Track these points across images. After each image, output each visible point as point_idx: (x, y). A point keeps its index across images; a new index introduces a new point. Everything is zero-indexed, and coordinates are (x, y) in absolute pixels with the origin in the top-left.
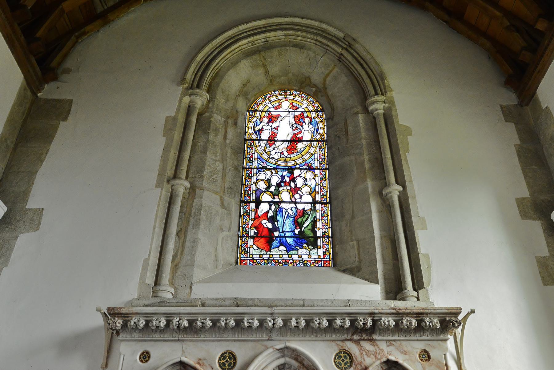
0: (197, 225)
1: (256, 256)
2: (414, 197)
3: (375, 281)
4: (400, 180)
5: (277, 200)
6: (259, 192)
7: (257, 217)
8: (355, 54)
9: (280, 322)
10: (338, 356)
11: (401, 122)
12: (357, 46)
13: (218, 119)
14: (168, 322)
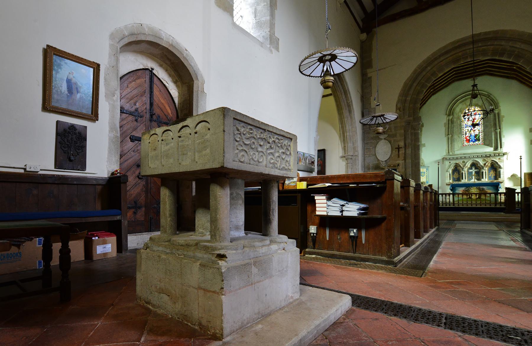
0: (454, 142)
1: (466, 144)
2: (503, 131)
3: (492, 147)
4: (500, 128)
5: (470, 133)
6: (466, 132)
7: (466, 137)
8: (491, 98)
11: (502, 115)
12: (491, 96)
13: (455, 120)
14: (453, 158)
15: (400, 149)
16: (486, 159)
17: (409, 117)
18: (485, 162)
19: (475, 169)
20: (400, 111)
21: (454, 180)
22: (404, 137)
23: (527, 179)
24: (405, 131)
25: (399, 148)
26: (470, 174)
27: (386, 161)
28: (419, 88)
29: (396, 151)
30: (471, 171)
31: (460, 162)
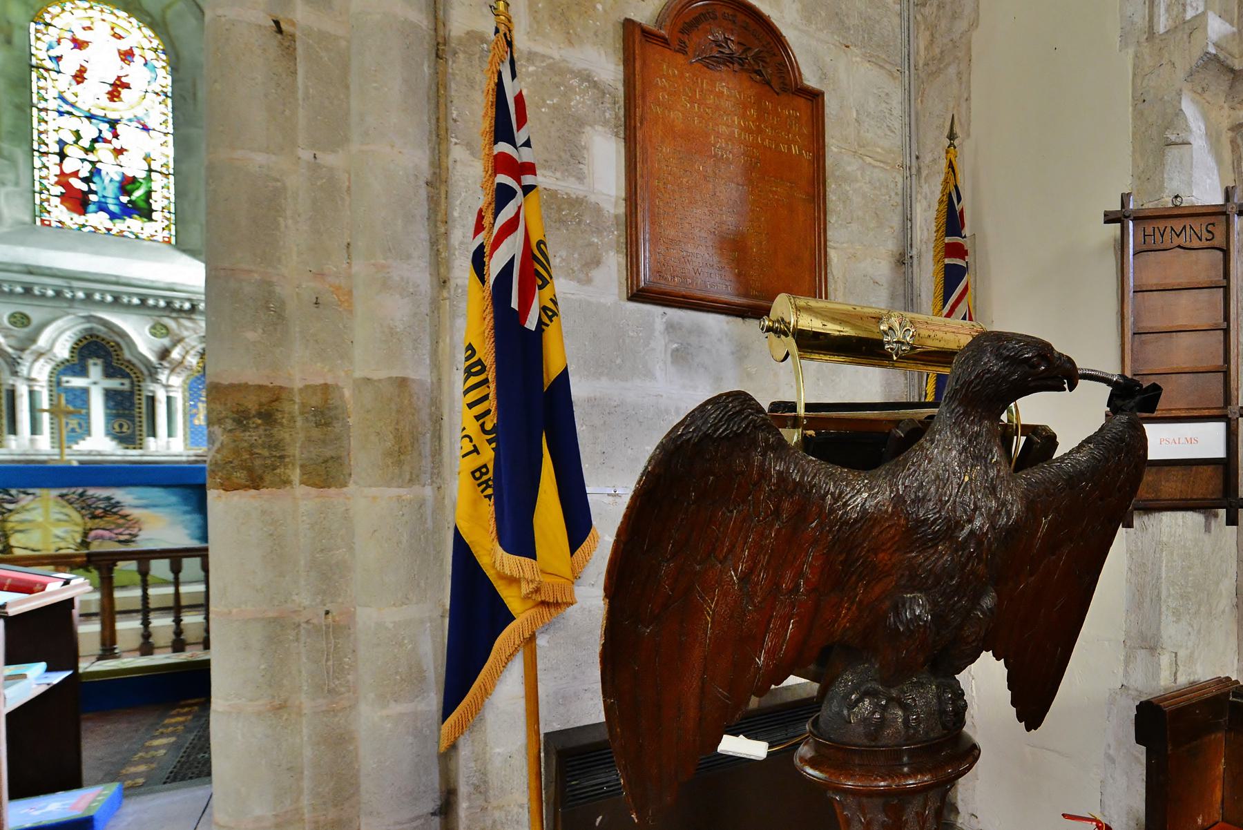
10: (153, 327)
16: (171, 324)
18: (166, 342)
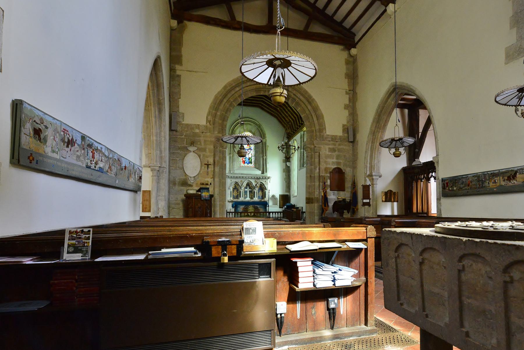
0: (234, 161)
1: (243, 165)
4: (266, 156)
9: (248, 177)
12: (261, 127)
15: (210, 166)
17: (218, 133)
18: (256, 183)
19: (249, 188)
20: (210, 124)
21: (234, 198)
22: (213, 154)
23: (281, 200)
24: (214, 147)
25: (208, 165)
26: (246, 192)
27: (194, 177)
28: (228, 106)
29: (204, 168)
30: (246, 190)
31: (238, 180)
